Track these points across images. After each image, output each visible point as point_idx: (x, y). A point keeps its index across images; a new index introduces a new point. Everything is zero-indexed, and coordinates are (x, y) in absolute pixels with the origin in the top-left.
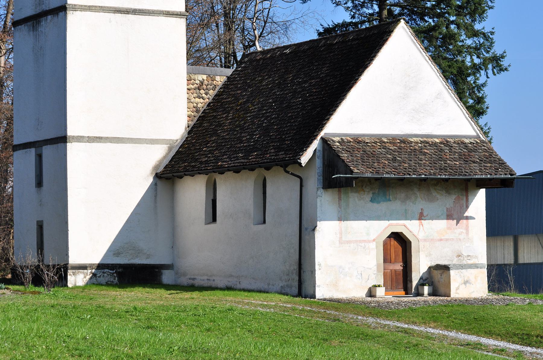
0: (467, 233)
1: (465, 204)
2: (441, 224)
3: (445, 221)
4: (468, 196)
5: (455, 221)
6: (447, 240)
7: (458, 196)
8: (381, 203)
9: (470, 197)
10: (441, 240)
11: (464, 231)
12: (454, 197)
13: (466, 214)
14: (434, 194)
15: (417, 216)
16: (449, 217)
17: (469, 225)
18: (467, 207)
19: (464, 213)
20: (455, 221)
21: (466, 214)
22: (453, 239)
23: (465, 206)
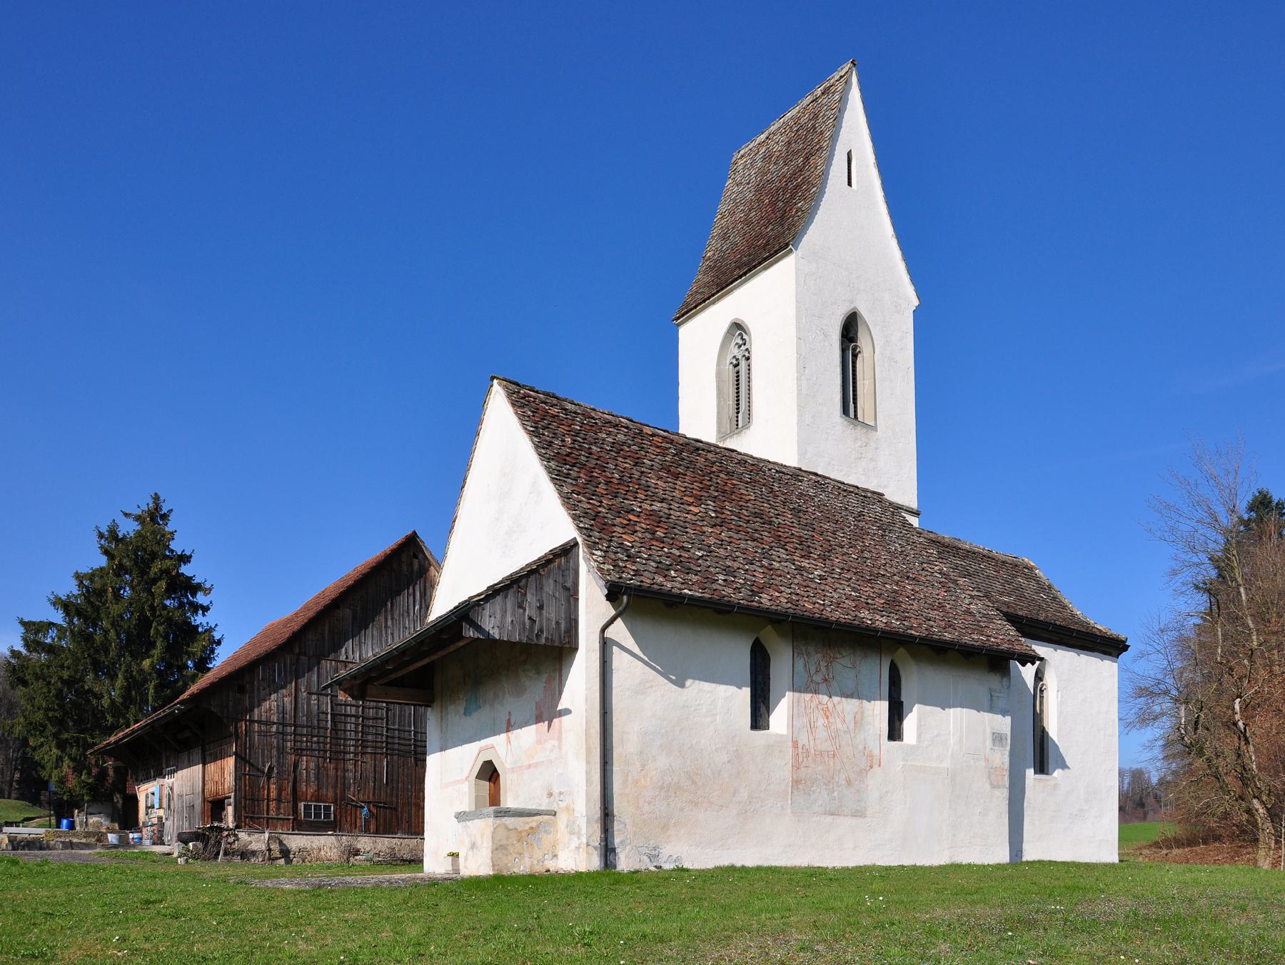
0: (560, 748)
1: (557, 688)
2: (528, 735)
3: (534, 727)
4: (561, 670)
5: (546, 723)
6: (537, 765)
7: (549, 675)
8: (473, 713)
9: (563, 672)
10: (529, 766)
11: (556, 743)
12: (544, 677)
13: (560, 707)
14: (522, 681)
15: (504, 726)
16: (538, 719)
17: (563, 730)
18: (560, 693)
19: (557, 707)
20: (546, 723)
21: (560, 707)
22: (543, 762)
23: (557, 692)
